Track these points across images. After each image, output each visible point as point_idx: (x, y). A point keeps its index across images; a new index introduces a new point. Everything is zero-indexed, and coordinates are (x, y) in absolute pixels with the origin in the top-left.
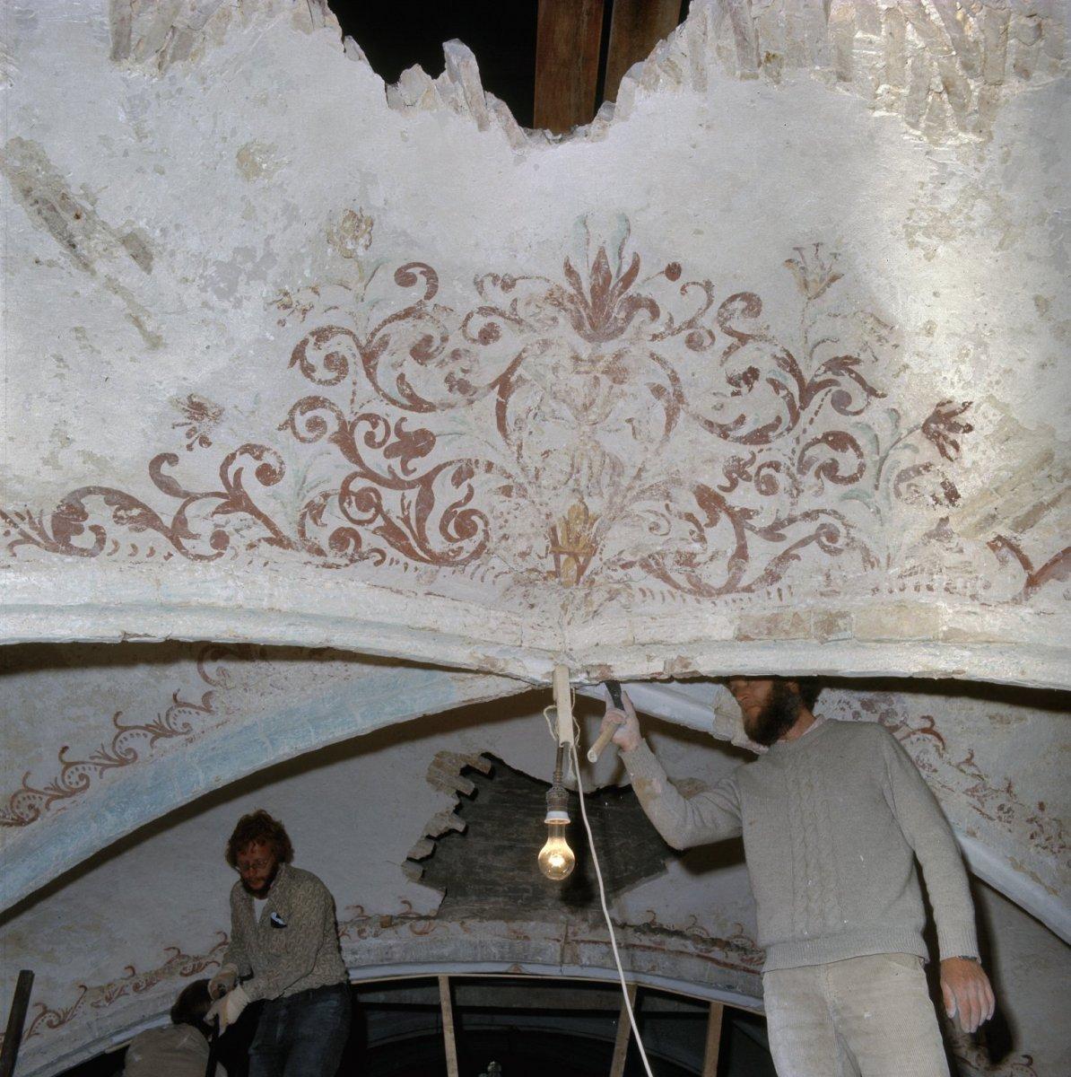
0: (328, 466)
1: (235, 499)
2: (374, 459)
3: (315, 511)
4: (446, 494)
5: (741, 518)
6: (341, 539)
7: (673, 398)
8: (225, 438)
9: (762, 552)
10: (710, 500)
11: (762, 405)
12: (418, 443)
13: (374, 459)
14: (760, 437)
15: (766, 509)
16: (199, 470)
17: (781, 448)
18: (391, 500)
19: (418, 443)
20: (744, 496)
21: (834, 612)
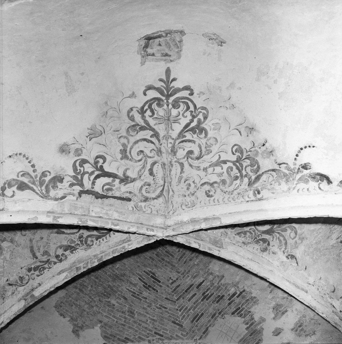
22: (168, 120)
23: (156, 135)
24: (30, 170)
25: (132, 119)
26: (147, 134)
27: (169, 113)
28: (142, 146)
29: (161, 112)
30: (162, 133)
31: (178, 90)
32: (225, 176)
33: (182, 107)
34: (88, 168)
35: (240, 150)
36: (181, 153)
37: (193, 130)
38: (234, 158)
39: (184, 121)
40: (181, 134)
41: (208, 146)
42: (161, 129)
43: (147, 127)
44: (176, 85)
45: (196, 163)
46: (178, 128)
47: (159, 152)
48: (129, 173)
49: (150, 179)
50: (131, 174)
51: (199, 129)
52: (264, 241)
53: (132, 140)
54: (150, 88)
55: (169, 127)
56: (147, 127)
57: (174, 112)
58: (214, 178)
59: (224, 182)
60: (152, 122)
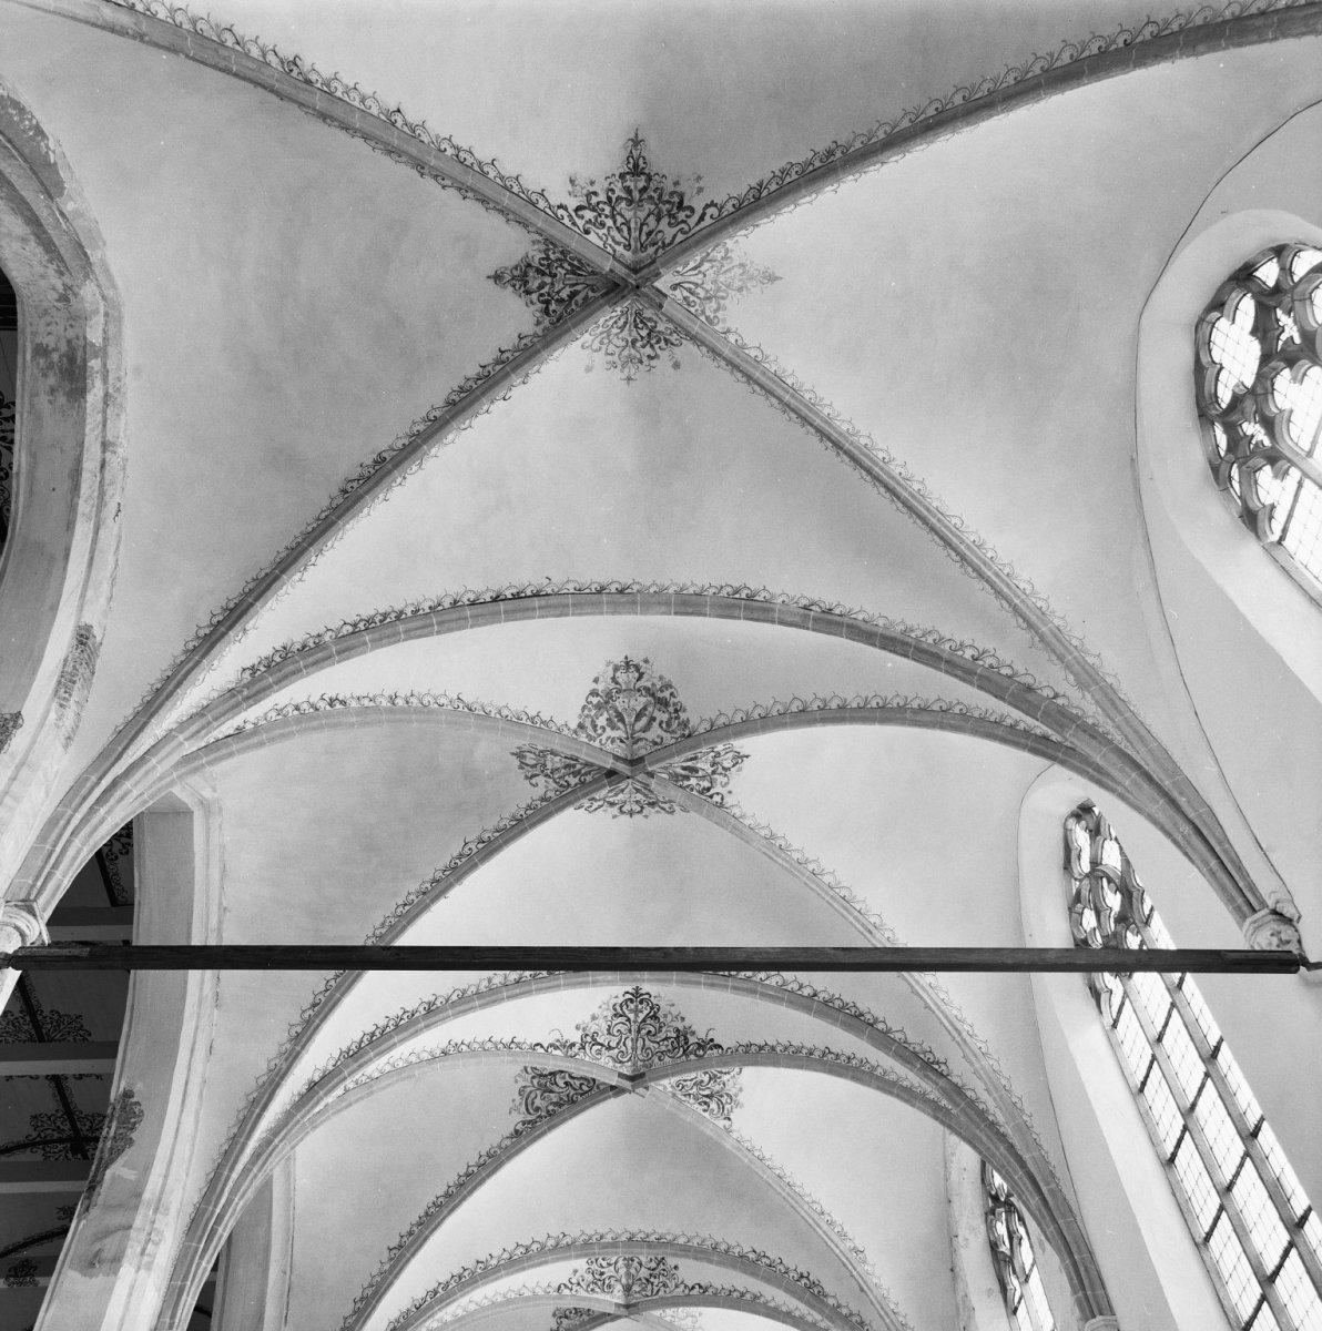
0: (590, 1278)
1: (579, 1284)
2: (597, 1276)
3: (588, 1286)
4: (607, 1282)
5: (652, 1283)
6: (592, 1290)
7: (640, 1264)
8: (578, 1274)
9: (656, 1289)
10: (647, 1280)
11: (653, 1265)
12: (602, 1274)
13: (597, 1276)
14: (654, 1269)
15: (656, 1281)
16: (574, 1281)
17: (656, 1272)
18: (599, 1283)
19: (602, 1274)
20: (652, 1280)
21: (772, 1304)
22: (636, 1011)
23: (629, 1020)
24: (560, 1038)
25: (615, 1010)
26: (623, 1019)
27: (637, 1006)
28: (620, 1027)
29: (632, 1006)
30: (632, 1019)
31: (642, 995)
32: (670, 1047)
33: (645, 1003)
34: (589, 1039)
35: (678, 1030)
36: (643, 1032)
37: (651, 1018)
38: (675, 1035)
39: (646, 1012)
40: (644, 1020)
41: (661, 1027)
42: (632, 1016)
43: (623, 1015)
44: (641, 992)
45: (653, 1038)
46: (642, 1016)
47: (630, 1031)
48: (611, 1044)
49: (623, 1049)
50: (613, 1044)
51: (655, 1017)
52: (706, 1103)
53: (614, 1023)
54: (627, 993)
55: (637, 1016)
56: (623, 1015)
57: (640, 1007)
58: (663, 1048)
59: (669, 1051)
60: (627, 1012)
